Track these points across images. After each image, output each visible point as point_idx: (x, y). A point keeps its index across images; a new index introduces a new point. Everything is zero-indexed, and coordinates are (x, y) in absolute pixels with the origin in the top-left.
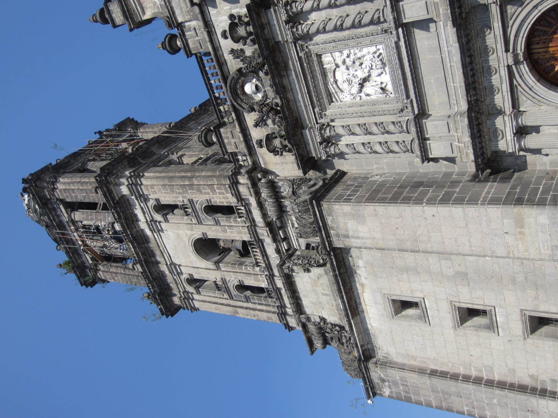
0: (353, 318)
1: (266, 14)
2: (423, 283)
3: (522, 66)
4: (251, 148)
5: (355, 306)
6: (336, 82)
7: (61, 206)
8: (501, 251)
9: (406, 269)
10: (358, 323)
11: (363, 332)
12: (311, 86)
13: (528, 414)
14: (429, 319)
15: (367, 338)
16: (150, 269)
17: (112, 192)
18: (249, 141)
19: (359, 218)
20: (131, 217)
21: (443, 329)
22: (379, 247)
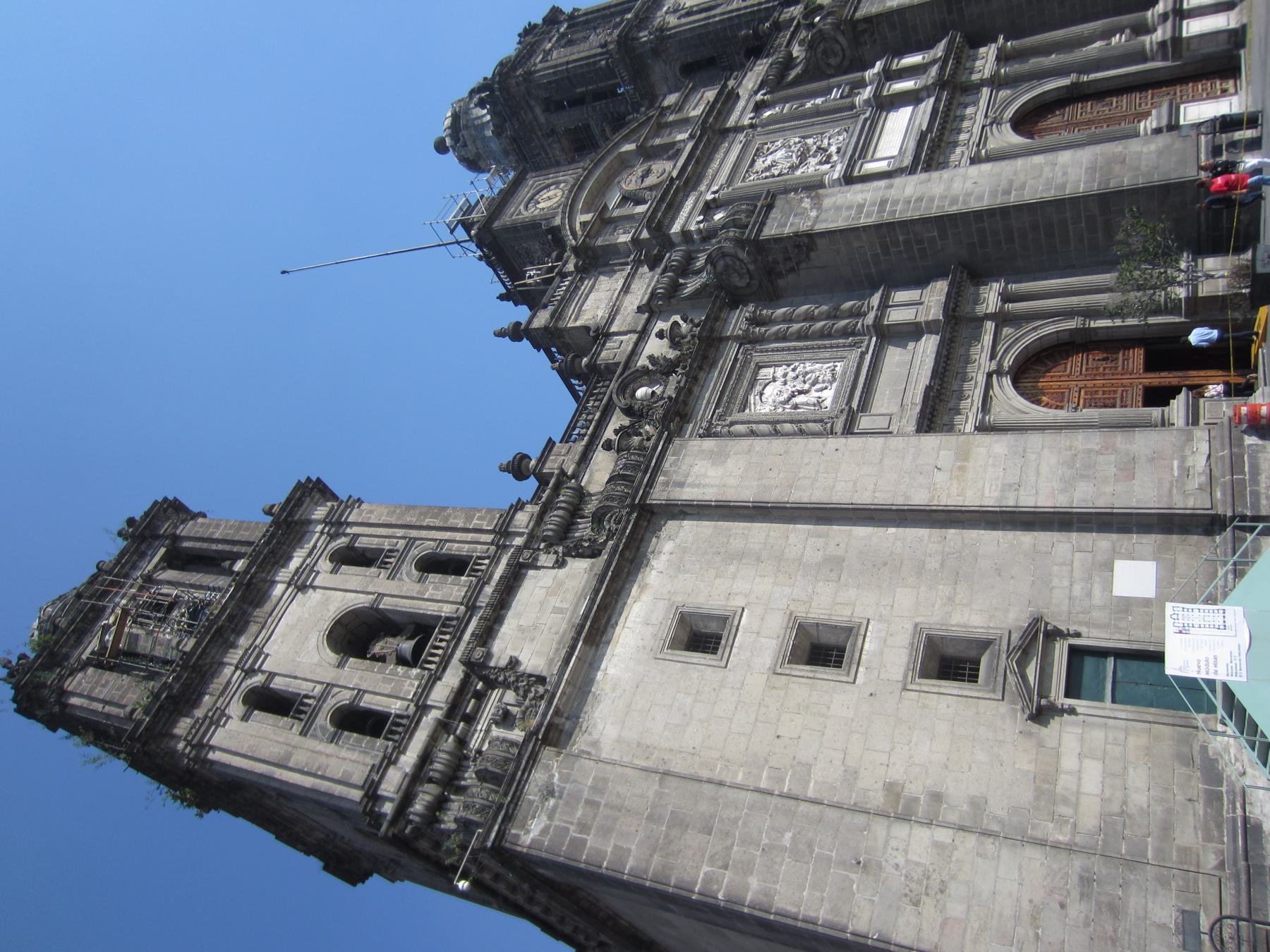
0: (585, 642)
1: (729, 313)
2: (758, 579)
3: (1004, 379)
4: (586, 460)
6: (761, 394)
7: (163, 550)
8: (919, 498)
9: (740, 556)
10: (585, 662)
11: (578, 686)
12: (725, 398)
13: (853, 876)
14: (731, 652)
15: (576, 703)
17: (301, 505)
19: (718, 458)
20: (281, 557)
21: (749, 673)
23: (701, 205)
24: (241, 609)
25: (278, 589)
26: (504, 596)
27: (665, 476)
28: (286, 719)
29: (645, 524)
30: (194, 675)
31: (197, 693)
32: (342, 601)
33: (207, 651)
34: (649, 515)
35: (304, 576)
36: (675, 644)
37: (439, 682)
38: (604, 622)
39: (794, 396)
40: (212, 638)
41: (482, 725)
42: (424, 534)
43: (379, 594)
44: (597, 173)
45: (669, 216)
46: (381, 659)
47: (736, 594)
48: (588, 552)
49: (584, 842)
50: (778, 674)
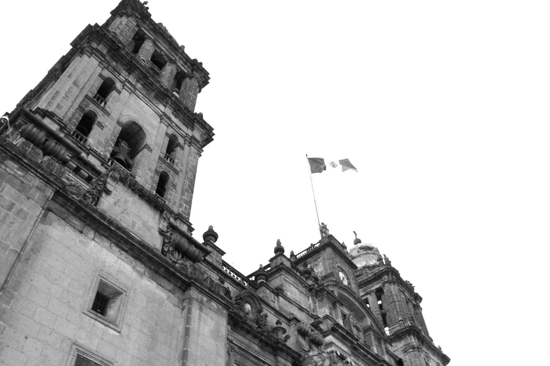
2: (137, 346)
5: (120, 244)
7: (186, 71)
9: (154, 338)
14: (92, 318)
16: (140, 72)
17: (202, 128)
18: (217, 272)
19: (215, 334)
20: (177, 114)
21: (75, 327)
22: (191, 333)
23: (345, 355)
24: (155, 89)
25: (162, 107)
26: (146, 198)
27: (207, 301)
28: (96, 92)
29: (179, 285)
30: (126, 61)
32: (151, 133)
33: (137, 70)
35: (167, 120)
36: (103, 285)
37: (100, 164)
38: (123, 246)
41: (72, 176)
44: (357, 304)
45: (339, 337)
46: (117, 144)
47: (129, 330)
48: (166, 249)
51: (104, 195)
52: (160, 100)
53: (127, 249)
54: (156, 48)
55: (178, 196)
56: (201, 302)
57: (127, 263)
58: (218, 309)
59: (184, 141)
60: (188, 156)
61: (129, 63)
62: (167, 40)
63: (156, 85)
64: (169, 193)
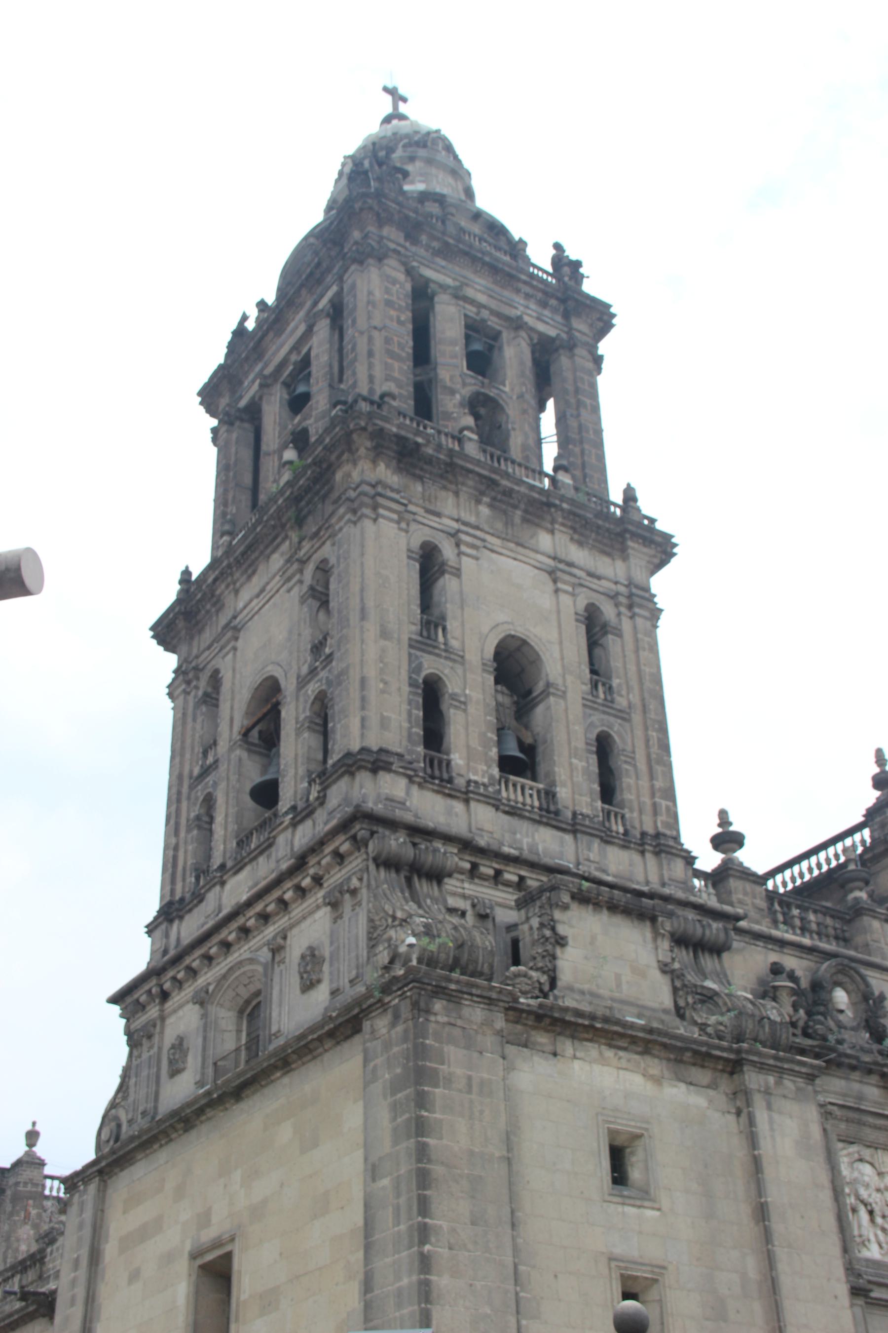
6: (861, 1160)
7: (552, 333)
16: (477, 478)
17: (645, 546)
18: (764, 942)
20: (581, 534)
24: (519, 502)
25: (545, 540)
28: (419, 611)
29: (720, 1067)
31: (421, 473)
33: (470, 475)
34: (729, 1069)
35: (567, 577)
36: (612, 1134)
39: (866, 1205)
40: (485, 477)
41: (471, 888)
42: (639, 732)
43: (564, 692)
48: (682, 1003)
49: (436, 1086)
50: (609, 1265)
51: (558, 951)
52: (536, 520)
53: (626, 1045)
54: (464, 308)
55: (644, 783)
56: (767, 1092)
57: (632, 1071)
58: (799, 1089)
59: (617, 605)
60: (637, 650)
61: (449, 469)
62: (485, 264)
63: (518, 492)
64: (624, 785)
